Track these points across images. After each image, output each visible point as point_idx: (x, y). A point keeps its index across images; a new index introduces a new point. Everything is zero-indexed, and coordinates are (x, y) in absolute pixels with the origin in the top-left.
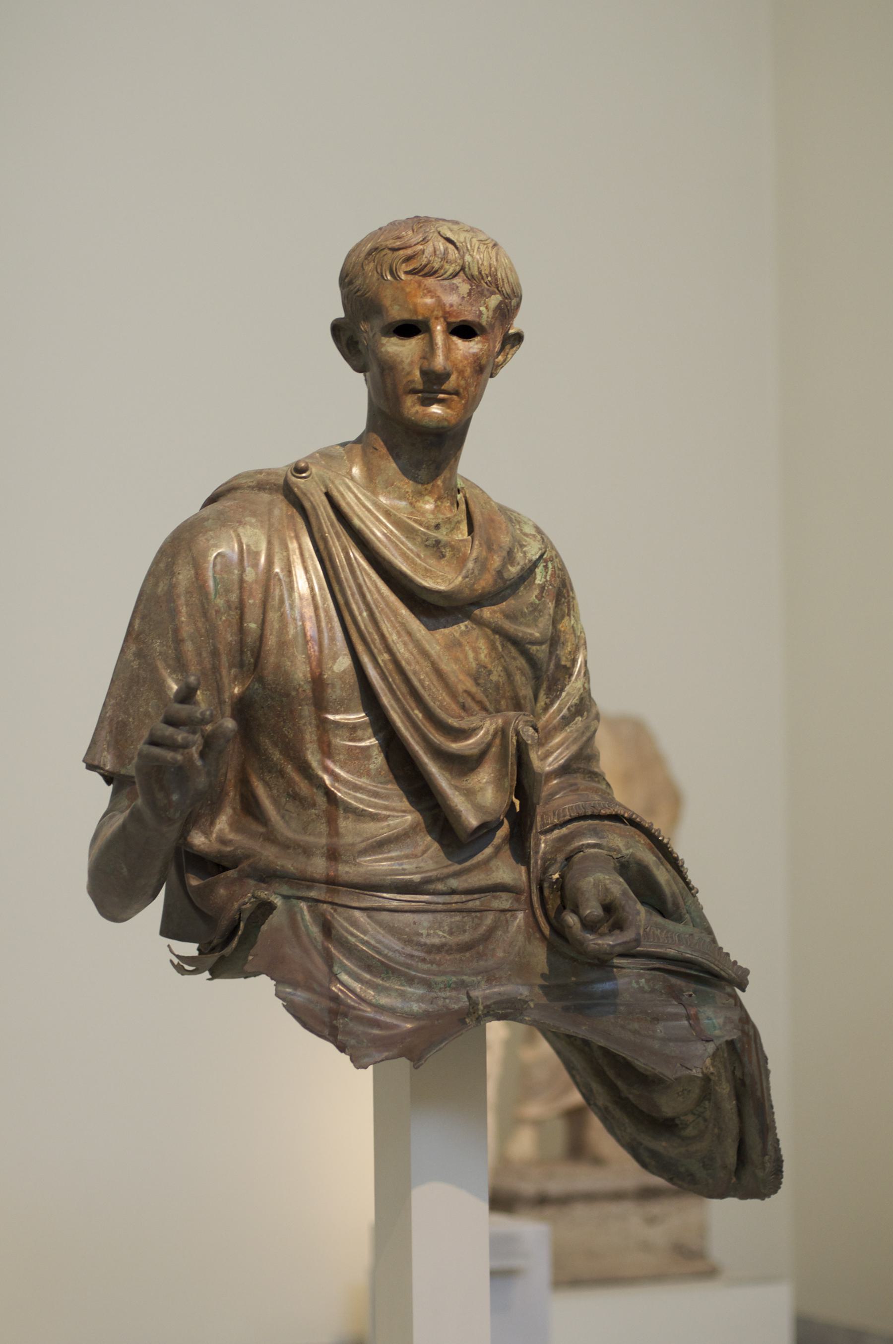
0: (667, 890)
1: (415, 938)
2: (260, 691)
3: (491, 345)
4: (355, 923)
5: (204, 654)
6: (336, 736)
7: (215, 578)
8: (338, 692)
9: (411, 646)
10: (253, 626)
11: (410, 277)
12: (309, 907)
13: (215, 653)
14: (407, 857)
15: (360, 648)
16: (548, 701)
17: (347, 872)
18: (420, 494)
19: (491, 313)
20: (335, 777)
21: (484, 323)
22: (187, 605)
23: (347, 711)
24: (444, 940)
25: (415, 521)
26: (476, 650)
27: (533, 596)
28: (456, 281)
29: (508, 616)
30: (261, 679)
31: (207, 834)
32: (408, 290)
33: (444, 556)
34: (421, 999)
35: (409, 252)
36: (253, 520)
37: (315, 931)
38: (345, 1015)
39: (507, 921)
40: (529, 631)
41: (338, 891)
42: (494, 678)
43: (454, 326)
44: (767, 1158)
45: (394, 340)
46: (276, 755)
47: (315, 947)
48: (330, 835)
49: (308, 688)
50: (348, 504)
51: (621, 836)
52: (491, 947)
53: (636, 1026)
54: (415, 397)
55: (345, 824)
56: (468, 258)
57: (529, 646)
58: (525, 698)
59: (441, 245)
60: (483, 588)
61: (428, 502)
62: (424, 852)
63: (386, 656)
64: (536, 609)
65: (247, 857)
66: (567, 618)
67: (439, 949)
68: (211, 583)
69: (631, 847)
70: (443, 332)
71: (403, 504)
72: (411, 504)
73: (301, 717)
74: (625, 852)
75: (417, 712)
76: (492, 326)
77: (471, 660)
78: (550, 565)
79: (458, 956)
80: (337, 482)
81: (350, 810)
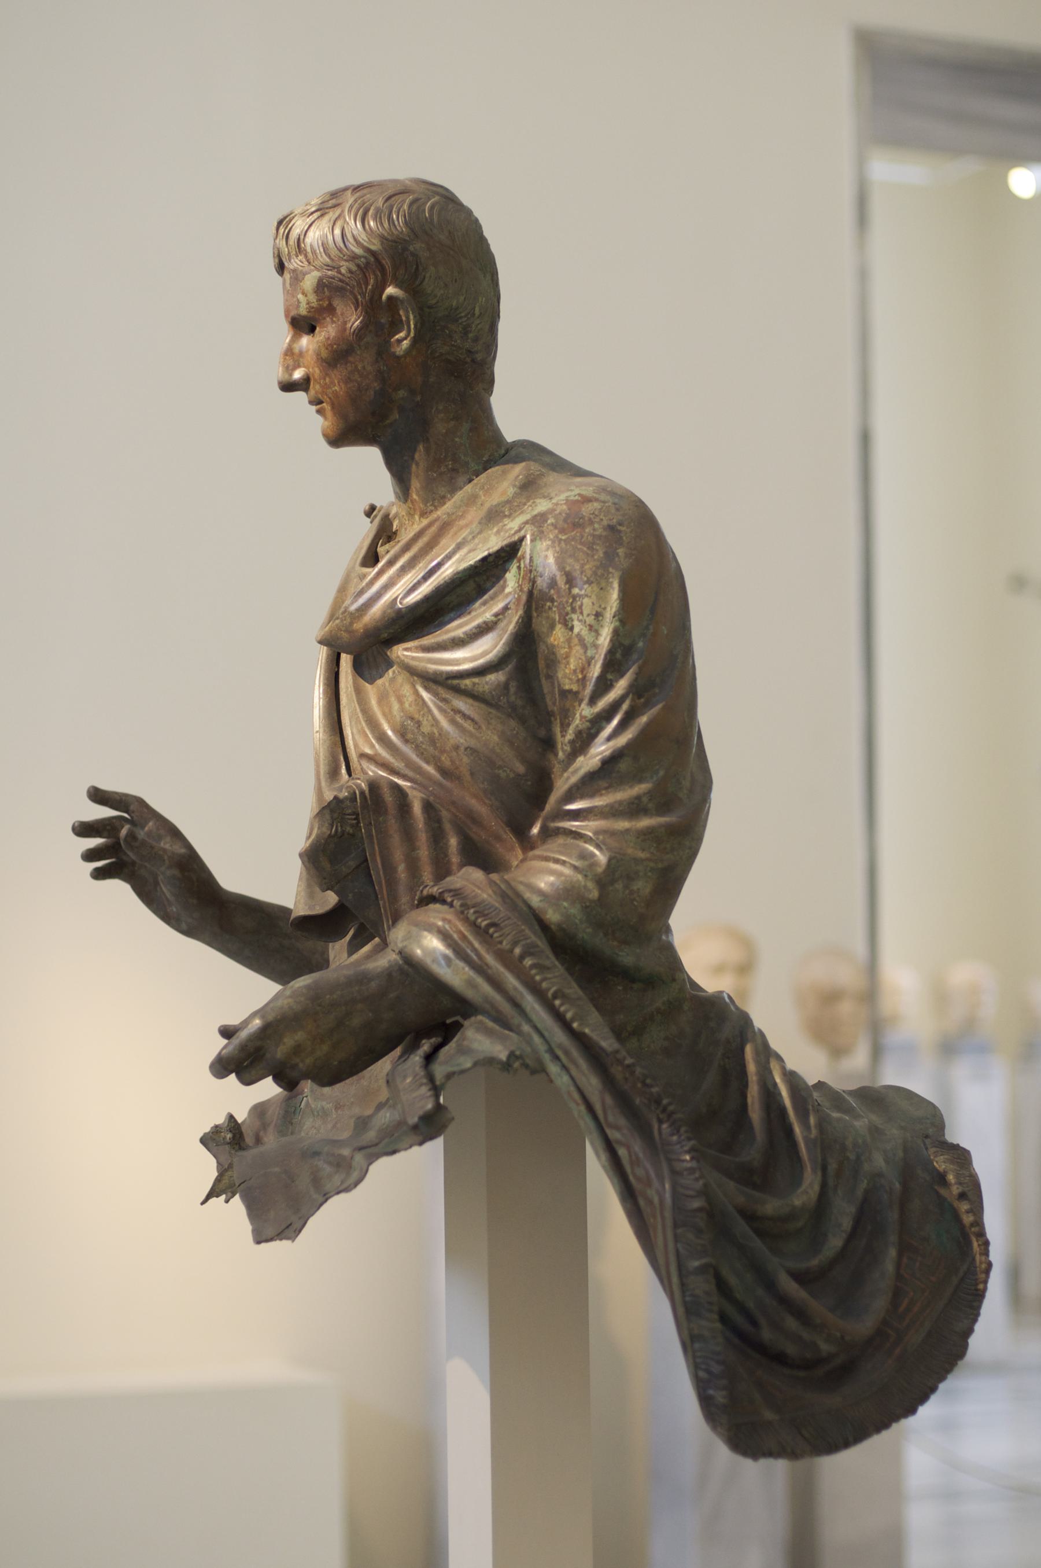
19: (313, 298)
57: (455, 682)
60: (366, 625)
76: (331, 310)
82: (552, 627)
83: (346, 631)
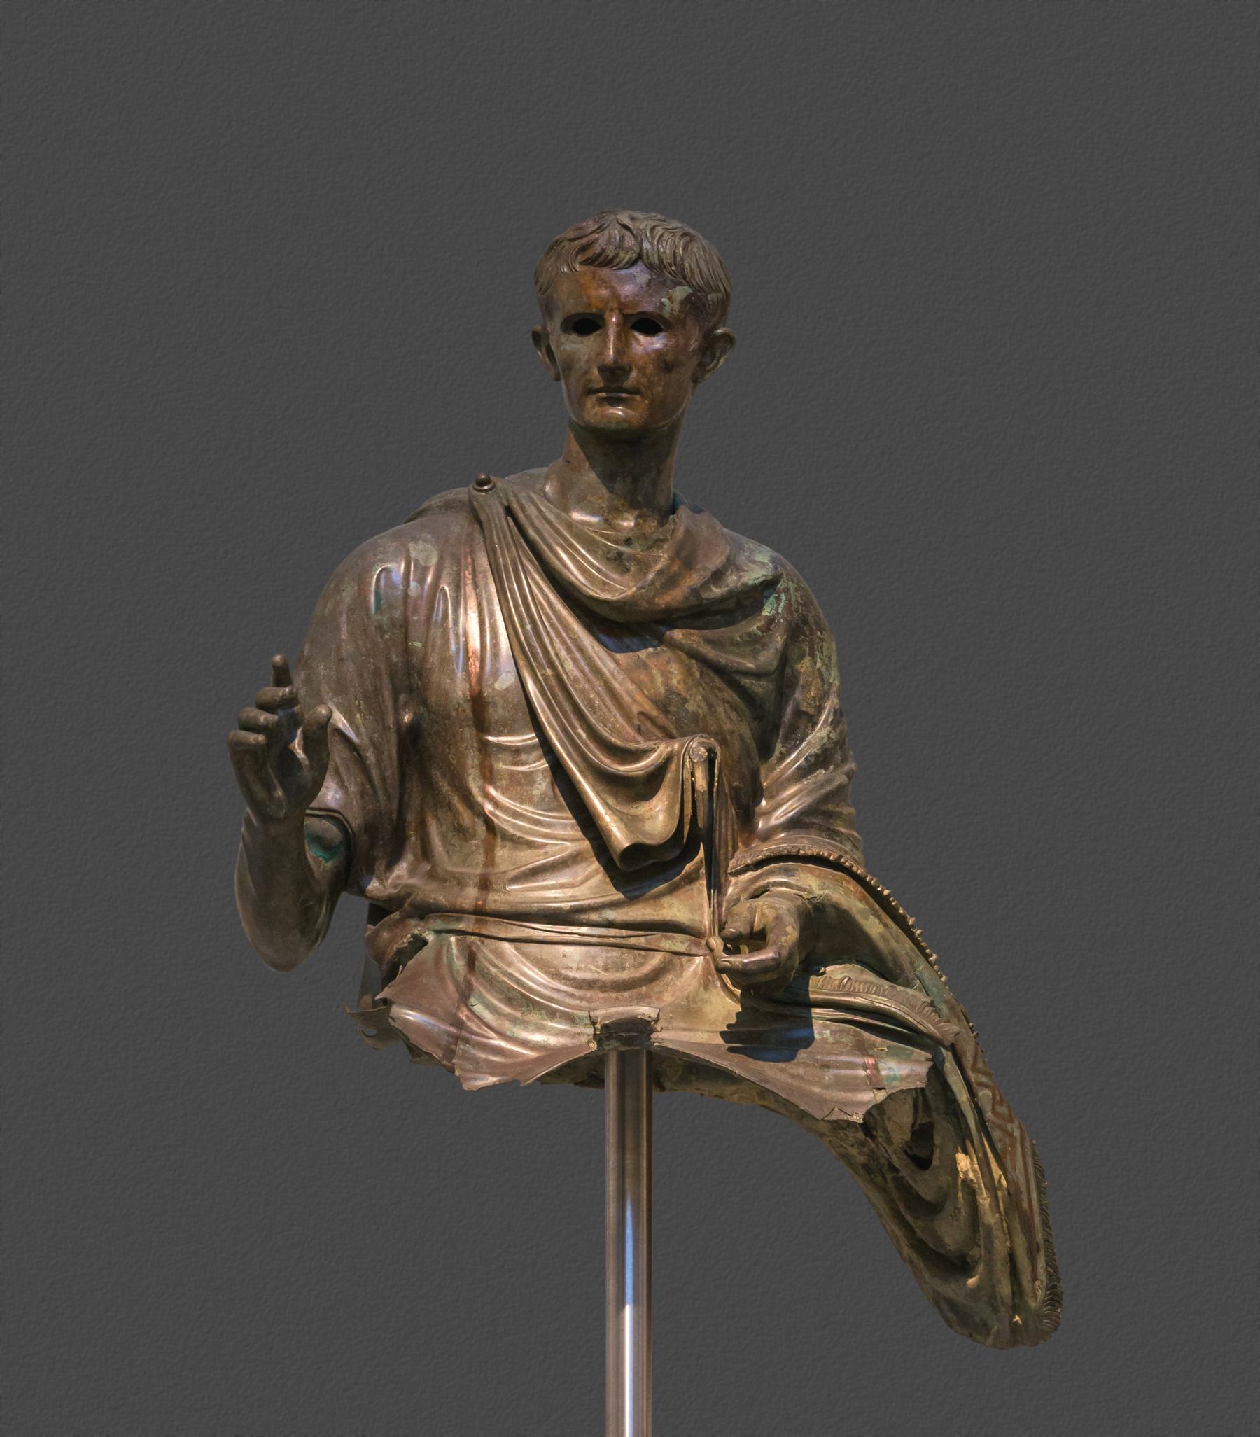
0: (882, 945)
1: (563, 972)
2: (426, 715)
3: (681, 342)
4: (500, 955)
5: (366, 675)
6: (498, 760)
7: (377, 594)
8: (500, 711)
9: (583, 663)
10: (418, 644)
11: (585, 268)
12: (458, 940)
13: (376, 674)
14: (562, 886)
15: (521, 663)
16: (784, 750)
17: (495, 901)
18: (617, 511)
19: (676, 306)
20: (496, 804)
21: (667, 316)
22: (349, 622)
23: (511, 733)
24: (596, 976)
25: (602, 535)
26: (666, 675)
27: (754, 627)
28: (633, 270)
29: (709, 641)
30: (424, 702)
31: (381, 881)
32: (582, 281)
33: (628, 570)
34: (562, 1033)
35: (584, 241)
36: (429, 537)
37: (460, 964)
38: (467, 1041)
39: (682, 965)
40: (740, 661)
41: (487, 921)
42: (691, 707)
43: (634, 320)
44: (1037, 1283)
45: (574, 337)
46: (445, 787)
47: (453, 976)
48: (486, 865)
49: (468, 707)
50: (528, 517)
51: (818, 876)
52: (657, 989)
53: (801, 1071)
54: (594, 397)
55: (502, 852)
56: (646, 245)
58: (732, 733)
59: (616, 232)
61: (627, 519)
62: (583, 882)
63: (549, 672)
64: (755, 643)
65: (409, 895)
66: (807, 660)
67: (590, 985)
68: (372, 599)
69: (828, 888)
70: (618, 325)
71: (594, 520)
72: (606, 520)
73: (463, 740)
74: (818, 892)
75: (580, 731)
77: (659, 684)
78: (783, 597)
79: (614, 995)
80: (520, 495)
81: (508, 838)
82: (802, 657)
83: (647, 602)
